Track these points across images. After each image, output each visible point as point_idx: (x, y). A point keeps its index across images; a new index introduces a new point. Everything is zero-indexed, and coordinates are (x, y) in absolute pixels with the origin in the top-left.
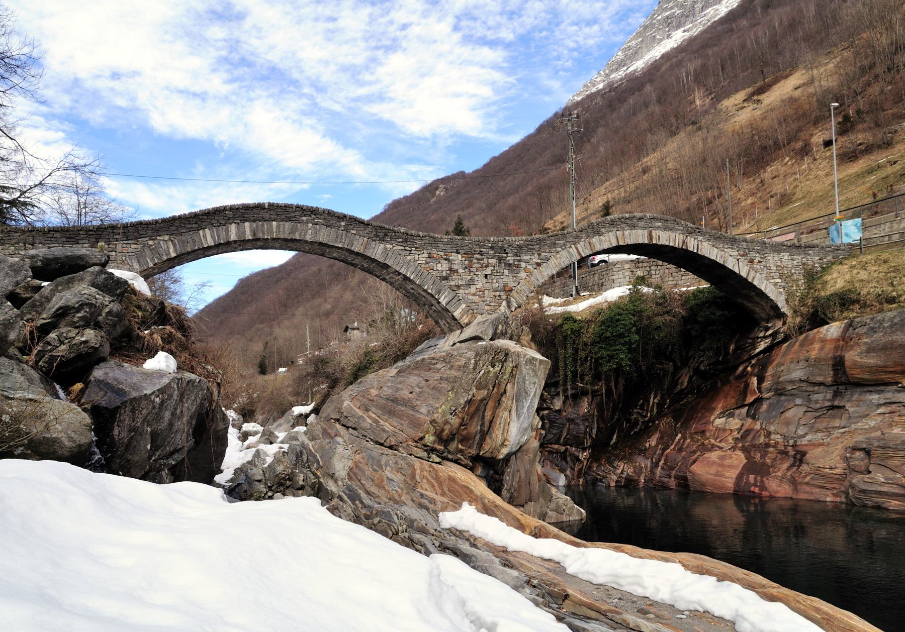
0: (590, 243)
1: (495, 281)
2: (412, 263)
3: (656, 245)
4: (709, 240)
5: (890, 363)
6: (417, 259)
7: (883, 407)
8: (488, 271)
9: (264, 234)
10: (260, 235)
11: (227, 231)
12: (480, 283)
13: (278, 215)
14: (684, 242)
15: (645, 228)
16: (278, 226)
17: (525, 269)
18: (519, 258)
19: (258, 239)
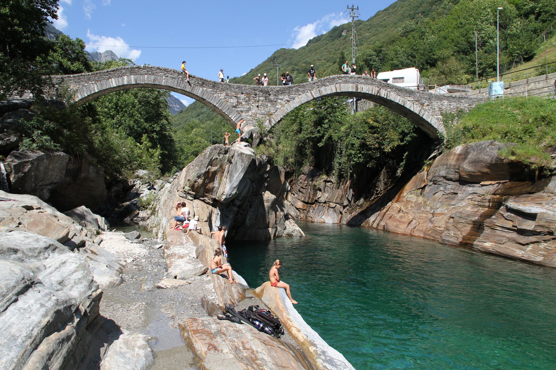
0: (319, 90)
1: (262, 109)
2: (217, 98)
3: (360, 92)
4: (395, 91)
5: (476, 171)
6: (219, 96)
7: (471, 195)
9: (140, 81)
10: (138, 82)
11: (123, 79)
12: (254, 110)
13: (148, 72)
14: (378, 92)
15: (354, 83)
16: (148, 78)
18: (277, 97)
19: (138, 84)
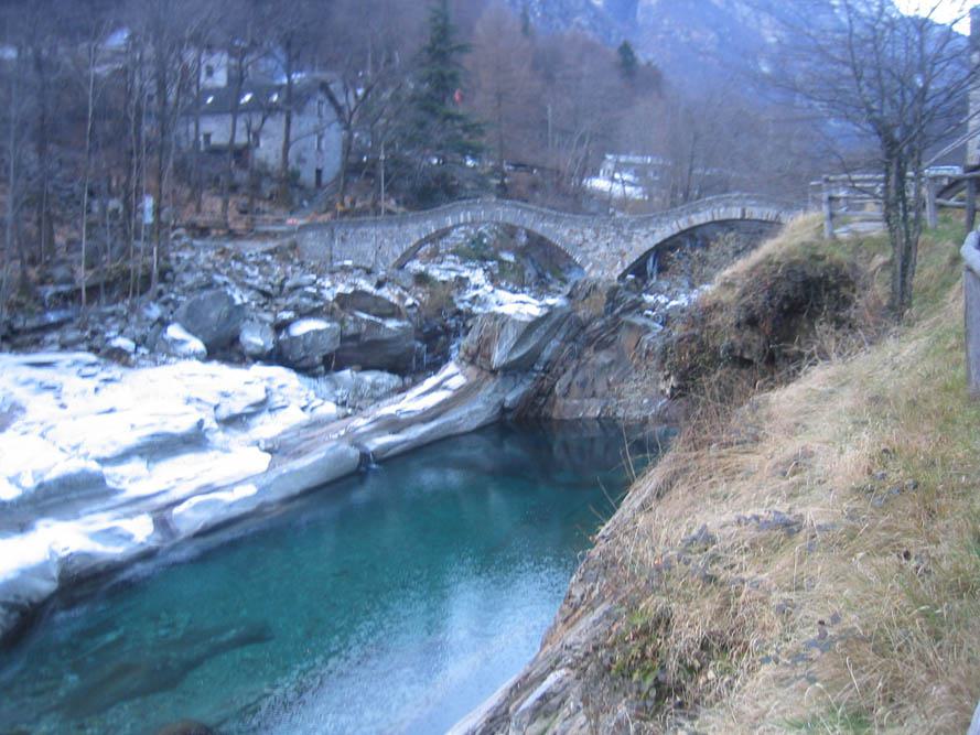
8: (609, 241)
12: (603, 250)
15: (739, 206)
17: (637, 240)
